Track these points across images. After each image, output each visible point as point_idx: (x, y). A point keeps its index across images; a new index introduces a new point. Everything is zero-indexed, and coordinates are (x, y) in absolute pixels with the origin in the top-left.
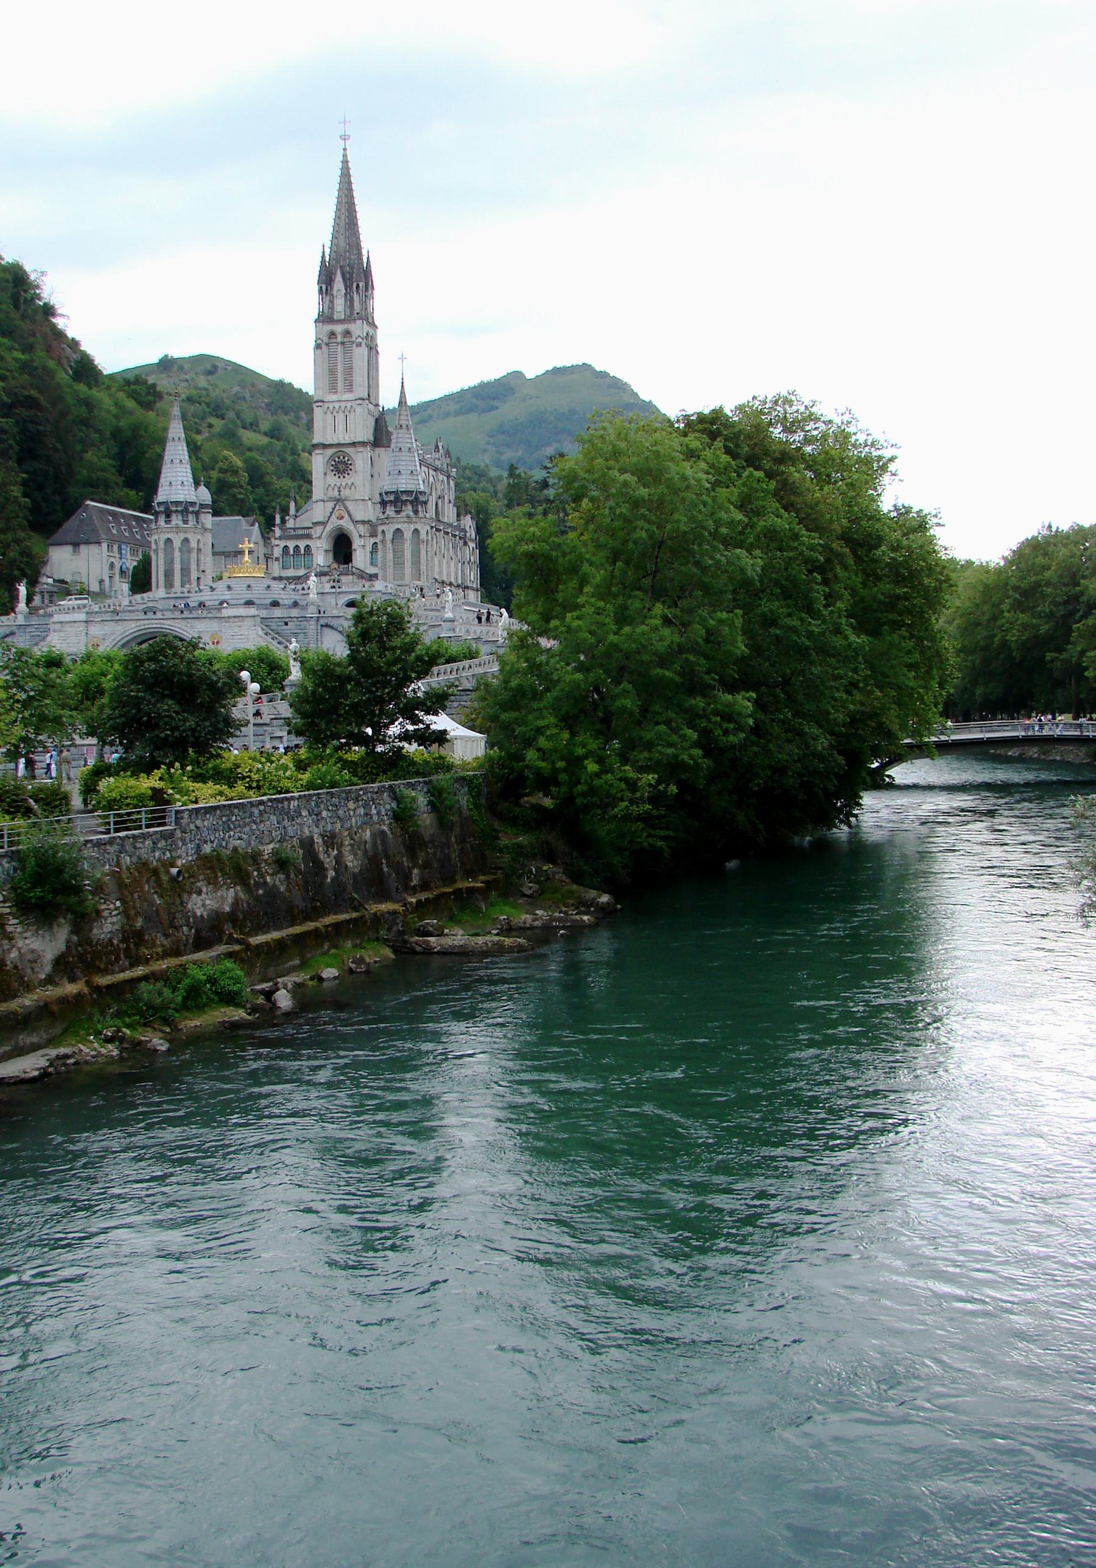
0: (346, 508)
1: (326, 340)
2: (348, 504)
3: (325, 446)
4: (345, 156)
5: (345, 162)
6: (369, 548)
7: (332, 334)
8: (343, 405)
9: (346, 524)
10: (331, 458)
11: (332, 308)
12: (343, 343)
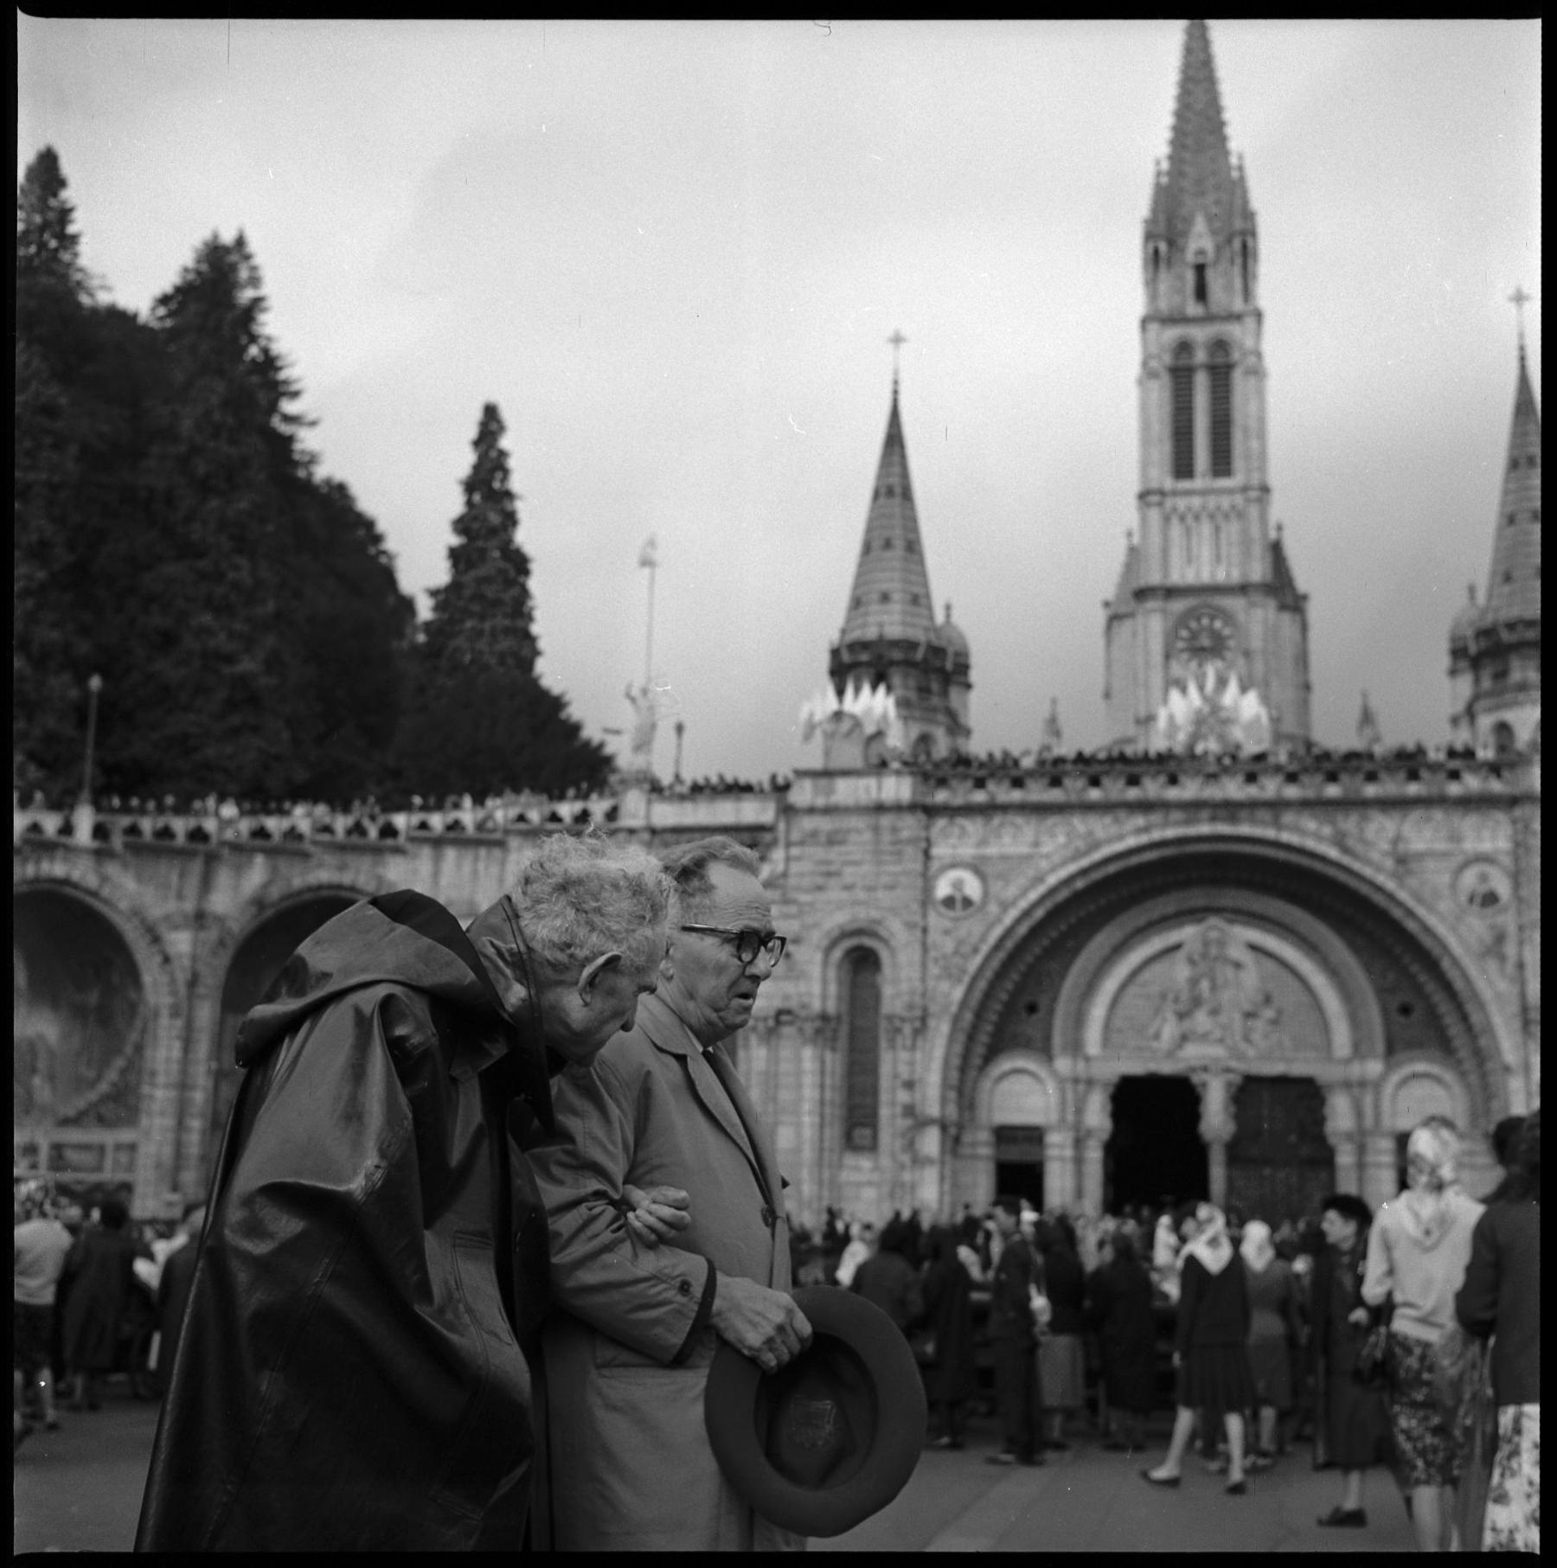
3: (1170, 592)
8: (1212, 502)
10: (1182, 620)
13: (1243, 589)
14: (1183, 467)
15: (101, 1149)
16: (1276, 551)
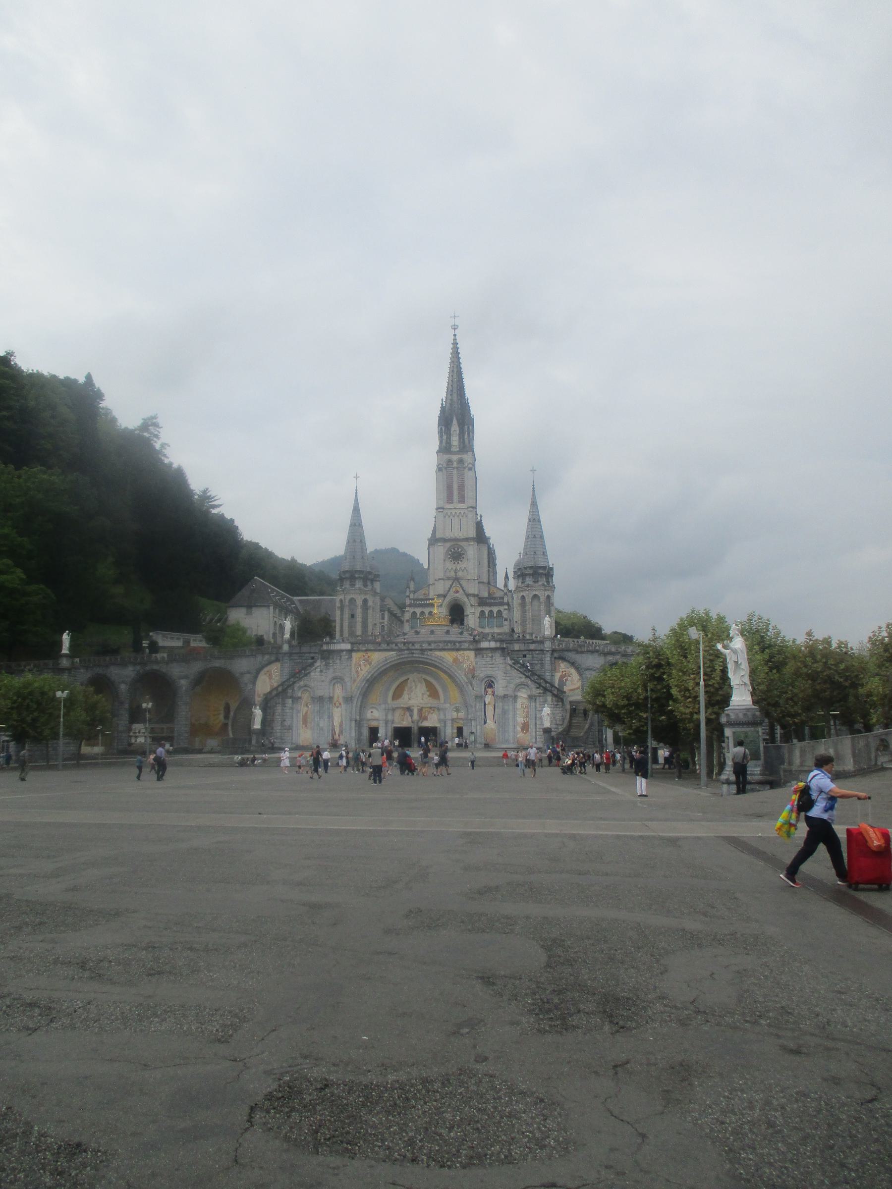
0: (461, 585)
1: (445, 465)
2: (462, 582)
3: (445, 540)
4: (455, 339)
5: (455, 344)
6: (477, 615)
7: (450, 462)
8: (458, 512)
9: (461, 596)
10: (449, 550)
11: (449, 442)
12: (457, 468)
13: (467, 540)
14: (450, 499)
15: (163, 728)
16: (479, 526)
